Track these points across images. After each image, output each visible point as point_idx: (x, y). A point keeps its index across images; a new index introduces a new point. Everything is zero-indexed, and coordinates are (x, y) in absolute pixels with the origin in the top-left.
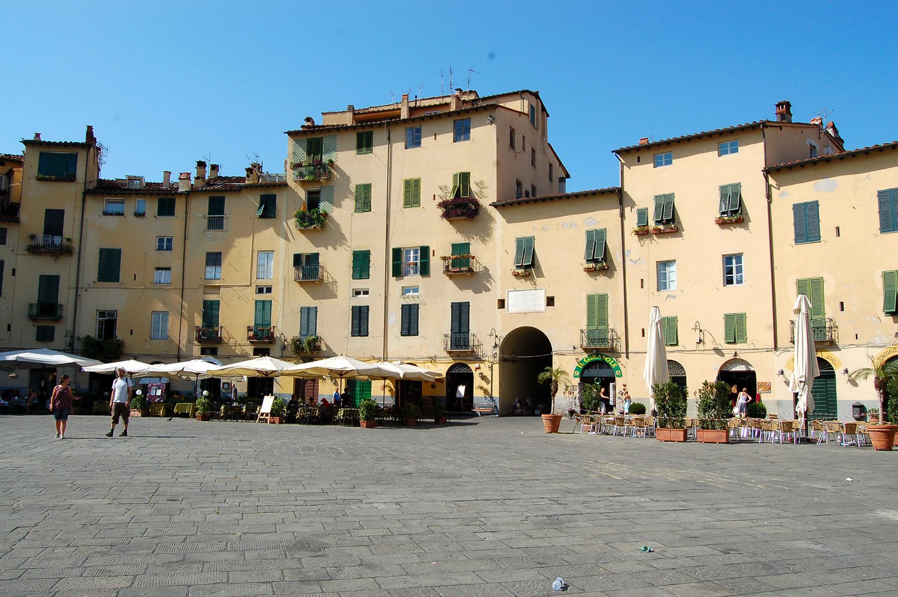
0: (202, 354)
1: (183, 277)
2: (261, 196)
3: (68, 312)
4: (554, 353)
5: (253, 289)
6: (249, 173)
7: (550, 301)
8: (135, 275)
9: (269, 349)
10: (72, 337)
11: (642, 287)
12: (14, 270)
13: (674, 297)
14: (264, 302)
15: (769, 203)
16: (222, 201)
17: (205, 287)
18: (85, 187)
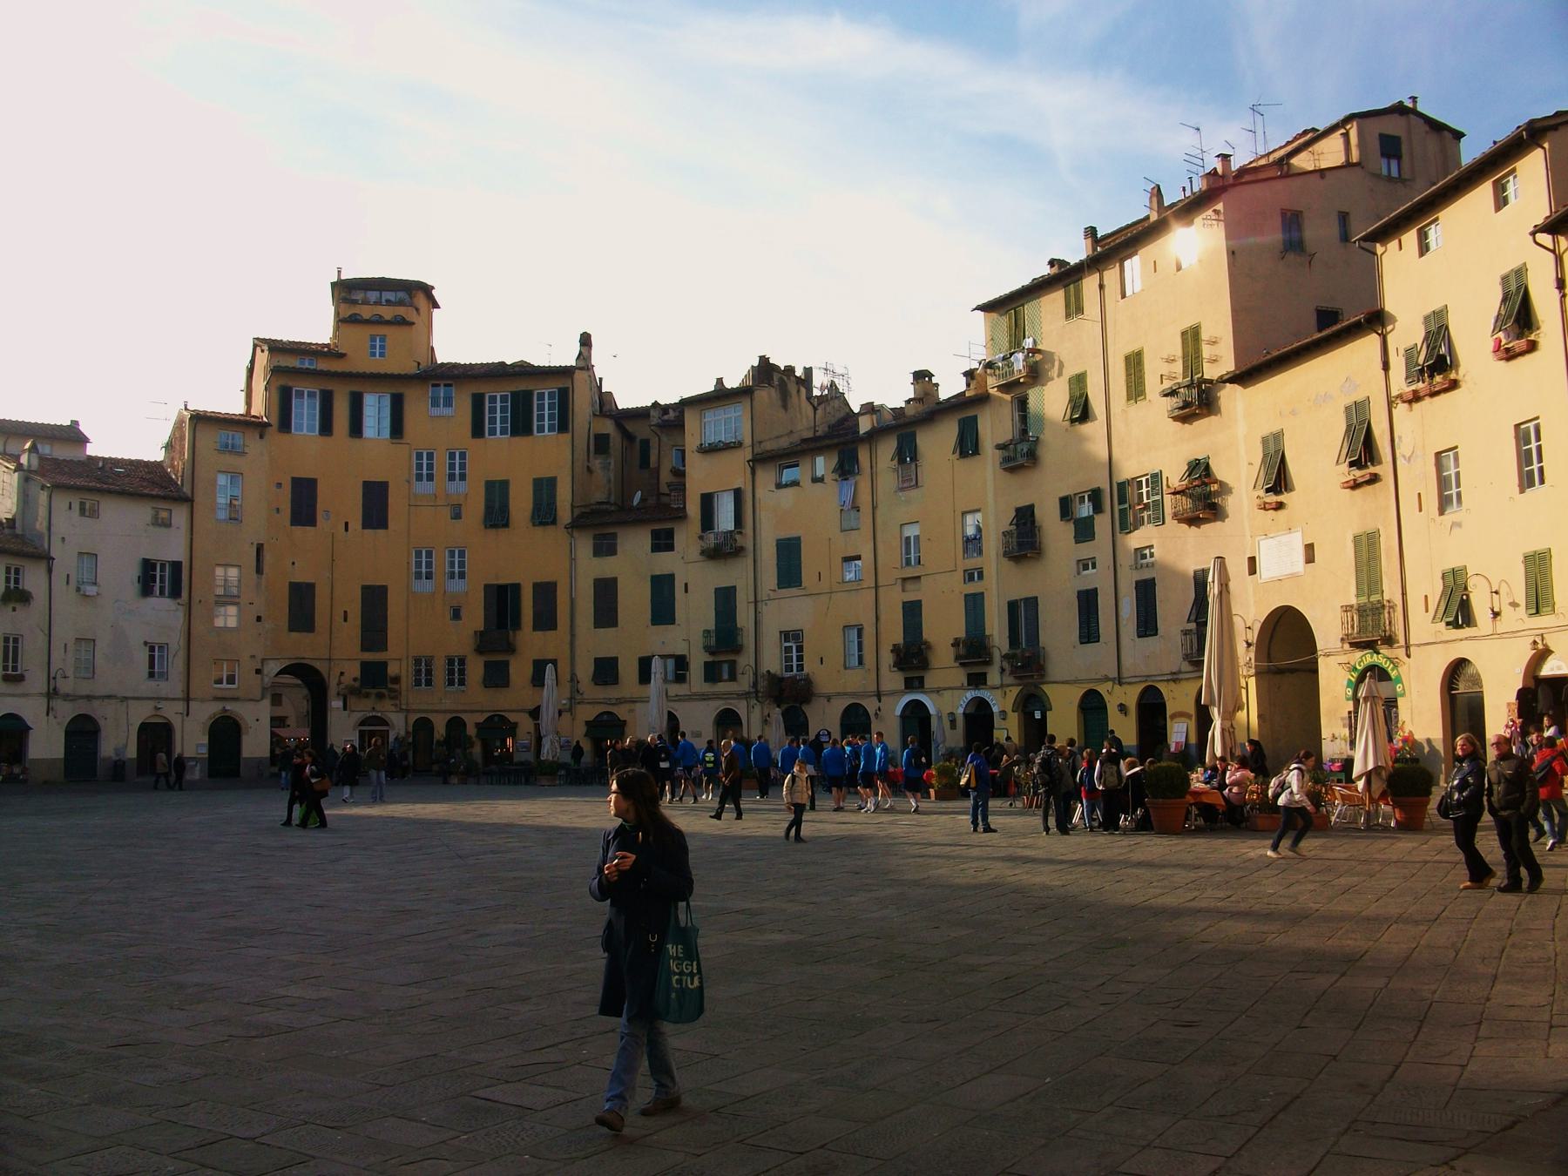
0: (906, 688)
1: (876, 569)
2: (959, 421)
3: (748, 640)
4: (1319, 653)
5: (959, 575)
6: (969, 379)
7: (1310, 553)
8: (820, 573)
9: (985, 674)
10: (756, 674)
11: (1420, 510)
12: (686, 585)
13: (1459, 525)
14: (974, 595)
15: (1564, 296)
16: (913, 436)
17: (904, 580)
18: (753, 452)
